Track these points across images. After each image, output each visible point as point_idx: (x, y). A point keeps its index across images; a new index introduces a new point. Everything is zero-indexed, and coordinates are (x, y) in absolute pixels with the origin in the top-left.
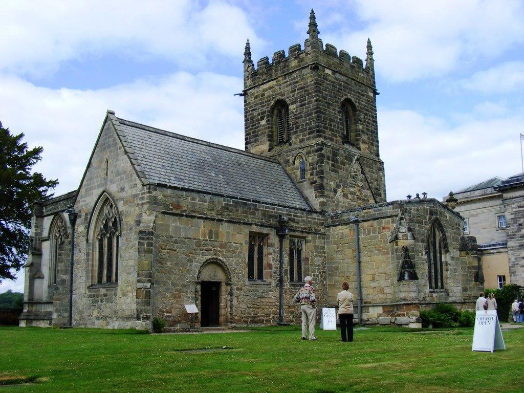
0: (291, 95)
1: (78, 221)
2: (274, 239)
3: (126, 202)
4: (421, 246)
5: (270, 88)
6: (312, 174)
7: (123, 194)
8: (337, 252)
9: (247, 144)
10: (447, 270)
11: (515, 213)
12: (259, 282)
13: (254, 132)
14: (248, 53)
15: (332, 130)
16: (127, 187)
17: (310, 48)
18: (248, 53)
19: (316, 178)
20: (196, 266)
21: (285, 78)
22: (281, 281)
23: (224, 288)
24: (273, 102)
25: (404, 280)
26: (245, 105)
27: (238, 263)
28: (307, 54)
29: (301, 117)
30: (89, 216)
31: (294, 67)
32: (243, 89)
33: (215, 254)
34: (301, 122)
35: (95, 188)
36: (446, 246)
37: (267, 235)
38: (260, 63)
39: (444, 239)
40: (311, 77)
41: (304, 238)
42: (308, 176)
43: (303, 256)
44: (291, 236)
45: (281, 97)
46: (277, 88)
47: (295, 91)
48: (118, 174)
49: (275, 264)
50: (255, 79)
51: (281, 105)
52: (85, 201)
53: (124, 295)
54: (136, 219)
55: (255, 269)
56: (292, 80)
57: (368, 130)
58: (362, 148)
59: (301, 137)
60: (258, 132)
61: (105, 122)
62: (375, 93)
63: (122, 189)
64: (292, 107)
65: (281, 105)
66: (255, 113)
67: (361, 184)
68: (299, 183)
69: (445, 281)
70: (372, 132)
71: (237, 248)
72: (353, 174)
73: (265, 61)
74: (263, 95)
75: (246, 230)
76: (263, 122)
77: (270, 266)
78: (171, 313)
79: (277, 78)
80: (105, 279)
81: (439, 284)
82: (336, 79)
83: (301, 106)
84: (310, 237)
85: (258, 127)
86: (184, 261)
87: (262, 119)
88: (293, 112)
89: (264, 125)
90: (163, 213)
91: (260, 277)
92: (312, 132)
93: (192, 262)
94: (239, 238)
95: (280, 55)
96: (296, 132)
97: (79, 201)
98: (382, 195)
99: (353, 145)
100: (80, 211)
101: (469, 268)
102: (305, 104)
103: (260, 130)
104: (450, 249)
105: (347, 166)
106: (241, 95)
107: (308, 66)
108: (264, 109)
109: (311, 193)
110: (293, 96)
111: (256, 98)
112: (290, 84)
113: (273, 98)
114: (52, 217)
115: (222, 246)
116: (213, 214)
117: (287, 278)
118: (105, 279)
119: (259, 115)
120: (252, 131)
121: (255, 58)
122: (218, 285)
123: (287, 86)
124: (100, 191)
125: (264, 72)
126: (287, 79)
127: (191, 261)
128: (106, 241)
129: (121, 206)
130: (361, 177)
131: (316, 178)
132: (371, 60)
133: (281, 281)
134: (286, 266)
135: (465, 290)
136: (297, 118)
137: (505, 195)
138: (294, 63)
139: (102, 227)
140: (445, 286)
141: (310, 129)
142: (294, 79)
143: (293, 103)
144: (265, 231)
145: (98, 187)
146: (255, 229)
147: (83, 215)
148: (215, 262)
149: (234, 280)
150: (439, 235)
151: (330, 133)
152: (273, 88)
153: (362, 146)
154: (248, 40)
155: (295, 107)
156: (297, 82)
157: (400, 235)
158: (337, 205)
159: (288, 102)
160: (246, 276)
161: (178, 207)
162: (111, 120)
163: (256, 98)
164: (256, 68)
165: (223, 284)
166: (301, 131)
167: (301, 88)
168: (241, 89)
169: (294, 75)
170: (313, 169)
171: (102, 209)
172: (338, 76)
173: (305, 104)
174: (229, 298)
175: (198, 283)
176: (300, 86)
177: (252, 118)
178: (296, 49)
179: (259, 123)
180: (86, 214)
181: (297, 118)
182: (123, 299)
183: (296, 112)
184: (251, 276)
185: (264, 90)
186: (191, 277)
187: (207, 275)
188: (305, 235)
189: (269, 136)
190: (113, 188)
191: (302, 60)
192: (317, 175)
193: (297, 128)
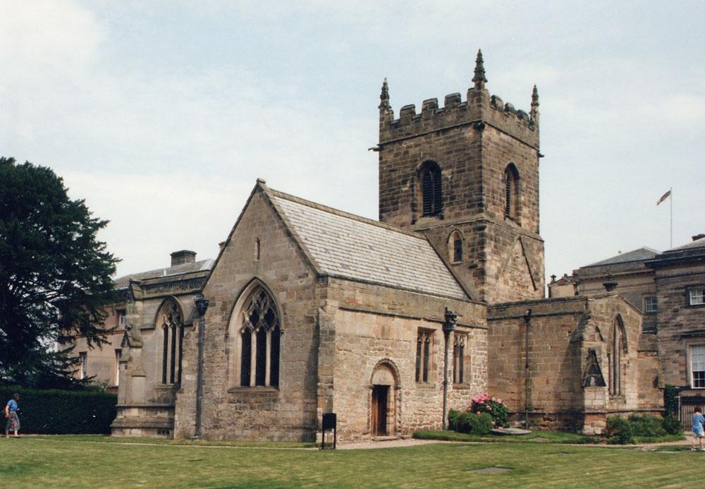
0: (446, 156)
1: (209, 309)
2: (440, 335)
4: (604, 346)
6: (470, 257)
8: (501, 349)
9: (381, 211)
10: (625, 374)
11: (670, 296)
12: (424, 384)
14: (385, 96)
15: (494, 204)
16: (291, 274)
18: (385, 96)
19: (476, 261)
20: (370, 366)
22: (445, 383)
23: (392, 392)
24: (419, 165)
25: (589, 385)
26: (381, 163)
27: (406, 364)
29: (457, 186)
30: (229, 306)
32: (378, 143)
33: (387, 354)
34: (458, 192)
35: (238, 272)
36: (625, 347)
37: (433, 331)
38: (403, 112)
39: (624, 339)
41: (467, 333)
42: (465, 257)
43: (465, 354)
44: (457, 332)
45: (431, 159)
47: (451, 152)
48: (276, 258)
49: (441, 364)
51: (430, 170)
52: (222, 286)
53: (289, 401)
54: (306, 315)
55: (422, 374)
56: (447, 138)
57: (529, 201)
58: (522, 225)
59: (457, 211)
60: (398, 198)
61: (254, 192)
62: (540, 156)
63: (285, 278)
65: (430, 170)
66: (394, 175)
67: (522, 268)
68: (453, 265)
69: (622, 386)
70: (534, 204)
71: (406, 346)
72: (514, 256)
73: (408, 110)
75: (415, 325)
77: (435, 366)
78: (346, 422)
80: (253, 382)
81: (617, 390)
82: (501, 139)
83: (459, 172)
84: (472, 332)
85: (398, 193)
86: (359, 362)
87: (404, 183)
88: (447, 179)
89: (406, 191)
90: (341, 308)
91: (425, 379)
92: (473, 206)
93: (365, 363)
94: (406, 333)
95: (431, 105)
96: (451, 204)
98: (542, 280)
99: (512, 219)
100: (213, 298)
101: (648, 371)
102: (464, 171)
104: (630, 348)
105: (508, 247)
106: (375, 150)
107: (470, 123)
109: (469, 280)
110: (448, 159)
111: (396, 155)
112: (445, 144)
115: (392, 345)
116: (385, 308)
117: (450, 379)
118: (253, 382)
119: (400, 177)
121: (396, 107)
122: (387, 387)
124: (248, 277)
126: (441, 136)
127: (364, 362)
128: (254, 338)
129: (281, 298)
130: (521, 259)
131: (476, 261)
132: (534, 112)
133: (445, 383)
134: (450, 367)
135: (641, 396)
136: (452, 187)
137: (658, 273)
139: (247, 319)
140: (623, 392)
141: (469, 202)
142: (451, 137)
143: (447, 168)
144: (431, 326)
145: (245, 271)
146: (425, 324)
147: (219, 304)
148: (387, 365)
149: (403, 384)
150: (619, 334)
151: (493, 207)
152: (419, 149)
153: (524, 221)
154: (385, 79)
156: (454, 142)
157: (586, 336)
158: (498, 294)
159: (441, 166)
160: (414, 378)
161: (354, 301)
162: (262, 190)
163: (396, 155)
164: (397, 116)
165: (392, 388)
166: (458, 203)
168: (375, 142)
169: (452, 133)
170: (473, 250)
171: (249, 296)
172: (502, 135)
173: (464, 171)
174: (398, 403)
175: (370, 388)
177: (390, 180)
178: (453, 99)
179: (400, 188)
180: (224, 304)
181: (452, 187)
182: (288, 406)
183: (452, 178)
184: (417, 380)
186: (365, 381)
187: (376, 381)
188: (468, 330)
189: (413, 205)
190: (269, 276)
192: (478, 258)
193: (453, 198)
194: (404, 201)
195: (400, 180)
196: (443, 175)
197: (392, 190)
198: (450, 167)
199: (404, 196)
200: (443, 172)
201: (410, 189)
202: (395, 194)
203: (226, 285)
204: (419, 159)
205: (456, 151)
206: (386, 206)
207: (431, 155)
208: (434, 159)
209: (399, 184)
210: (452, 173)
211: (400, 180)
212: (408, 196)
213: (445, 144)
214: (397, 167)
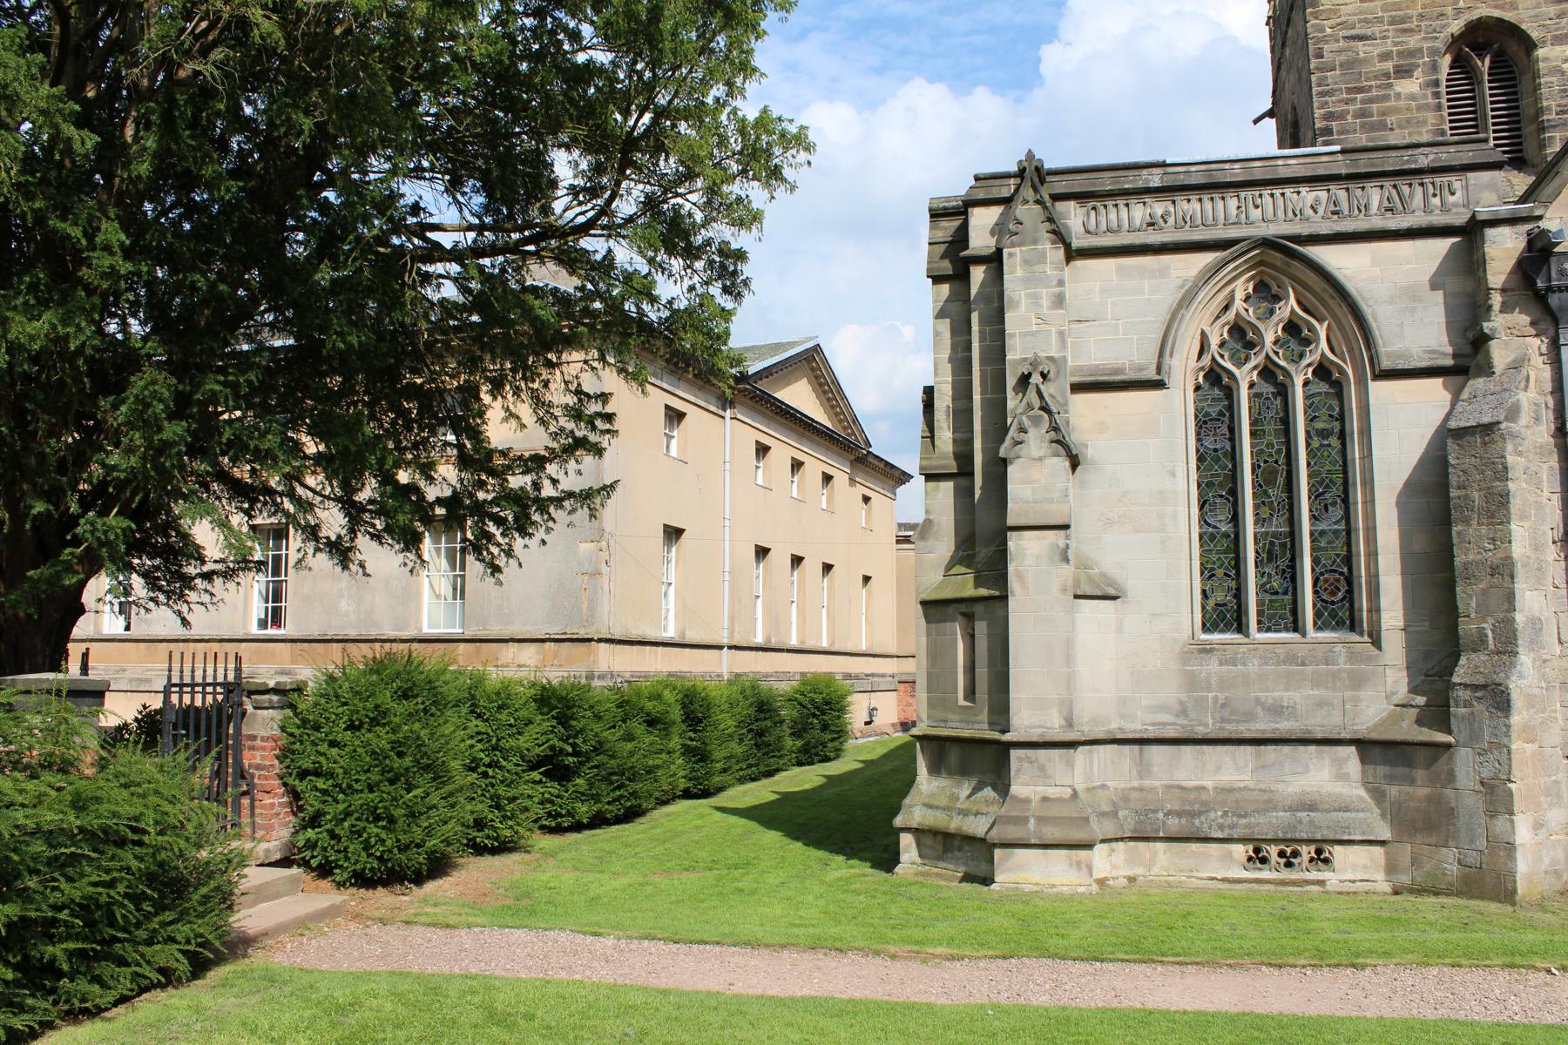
13: (1362, 114)
24: (1456, 26)
45: (1496, 13)
76: (1409, 86)
85: (1386, 98)
87: (1403, 72)
89: (1412, 97)
103: (1396, 110)
108: (1413, 42)
114: (1207, 258)
119: (1385, 57)
120: (1351, 108)
159: (1534, 35)
179: (1390, 86)
194: (1408, 121)
196: (1546, 59)
197: (1360, 90)
199: (1408, 109)
200: (1540, 52)
201: (1429, 92)
202: (1371, 101)
204: (1449, 10)
208: (1508, 16)
209: (1387, 75)
211: (1389, 66)
212: (1419, 108)
214: (1376, 30)
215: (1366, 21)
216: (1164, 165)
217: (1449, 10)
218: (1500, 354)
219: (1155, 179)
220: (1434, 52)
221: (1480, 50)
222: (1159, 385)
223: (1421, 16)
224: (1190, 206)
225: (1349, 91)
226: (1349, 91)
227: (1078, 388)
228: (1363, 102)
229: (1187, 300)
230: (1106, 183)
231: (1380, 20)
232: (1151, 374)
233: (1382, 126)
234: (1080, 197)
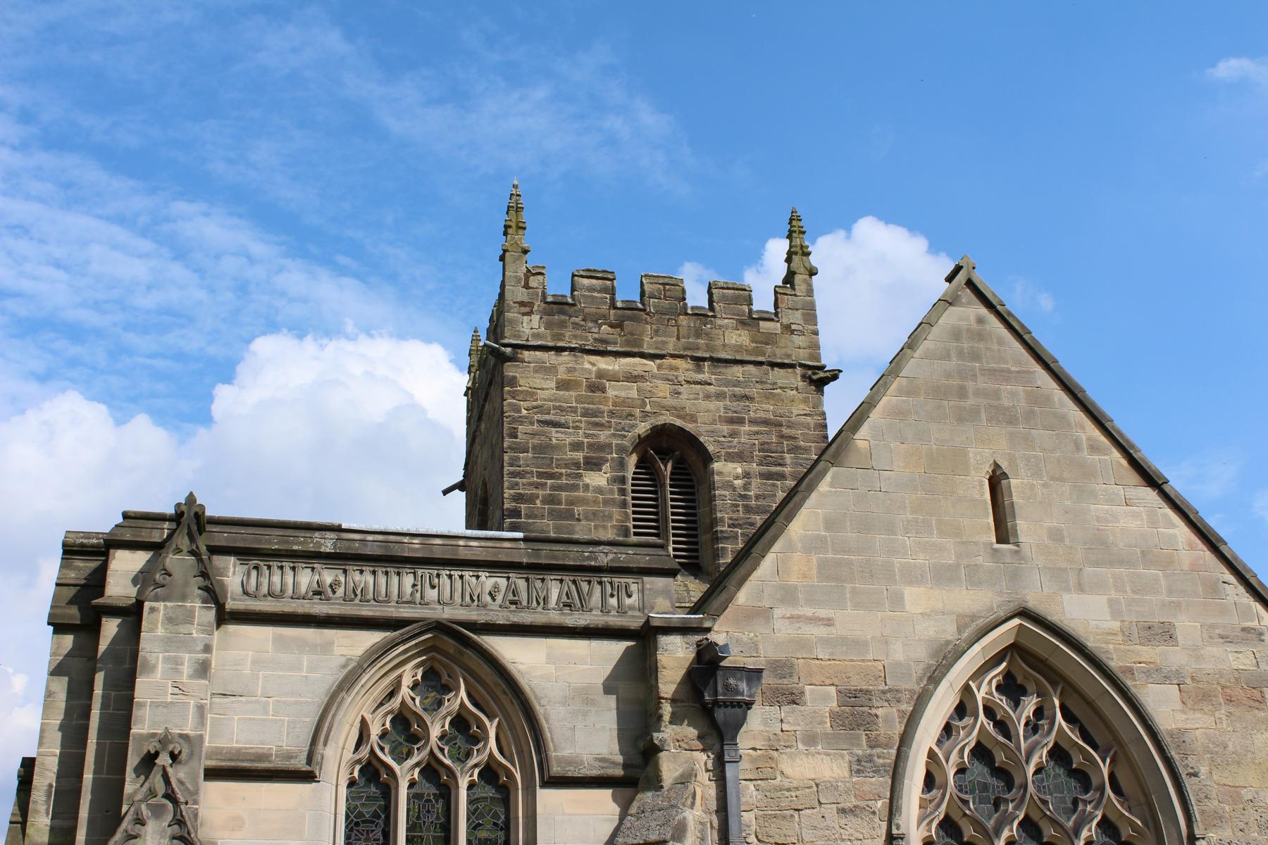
0: (725, 429)
1: (758, 724)
3: (1198, 694)
5: (632, 378)
7: (1175, 657)
13: (551, 500)
16: (1187, 626)
17: (798, 314)
21: (699, 369)
24: (643, 428)
28: (788, 329)
31: (739, 348)
35: (913, 577)
40: (806, 401)
45: (679, 423)
46: (663, 389)
47: (741, 421)
50: (562, 325)
52: (829, 622)
56: (727, 383)
64: (726, 470)
66: (555, 435)
74: (595, 388)
76: (598, 479)
79: (662, 357)
85: (575, 487)
87: (593, 464)
89: (599, 490)
97: (764, 614)
100: (783, 668)
103: (583, 501)
107: (792, 366)
108: (603, 436)
110: (733, 434)
111: (563, 385)
113: (645, 415)
114: (374, 638)
119: (577, 446)
120: (541, 493)
123: (708, 397)
124: (980, 600)
125: (604, 317)
138: (736, 339)
142: (737, 384)
143: (731, 457)
147: (821, 701)
155: (739, 470)
159: (711, 448)
167: (766, 422)
176: (762, 415)
179: (579, 476)
185: (601, 374)
190: (1087, 614)
191: (769, 339)
194: (594, 514)
195: (579, 456)
196: (720, 473)
197: (551, 476)
198: (738, 457)
199: (595, 502)
200: (716, 466)
203: (852, 621)
204: (637, 412)
205: (753, 422)
206: (528, 517)
207: (679, 411)
208: (689, 427)
209: (577, 465)
210: (747, 475)
212: (606, 502)
213: (720, 396)
214: (570, 418)
215: (561, 409)
216: (338, 529)
217: (637, 412)
218: (669, 768)
219: (328, 544)
220: (621, 449)
221: (664, 454)
222: (307, 777)
223: (612, 413)
224: (364, 578)
225: (540, 475)
226: (540, 475)
227: (213, 774)
228: (553, 488)
229: (348, 682)
230: (273, 541)
231: (574, 410)
232: (300, 764)
233: (569, 515)
234: (243, 553)
